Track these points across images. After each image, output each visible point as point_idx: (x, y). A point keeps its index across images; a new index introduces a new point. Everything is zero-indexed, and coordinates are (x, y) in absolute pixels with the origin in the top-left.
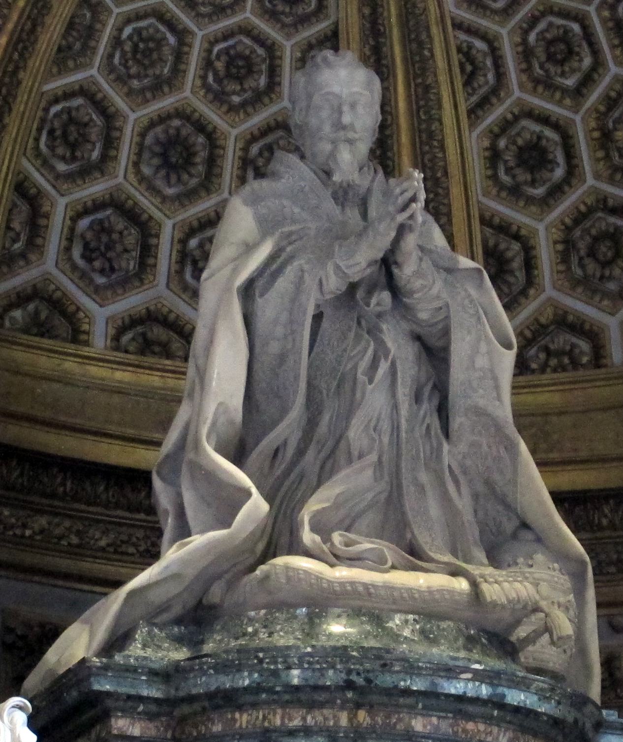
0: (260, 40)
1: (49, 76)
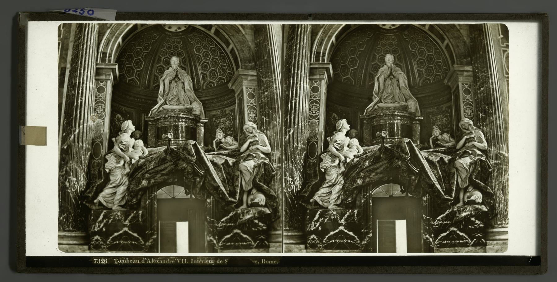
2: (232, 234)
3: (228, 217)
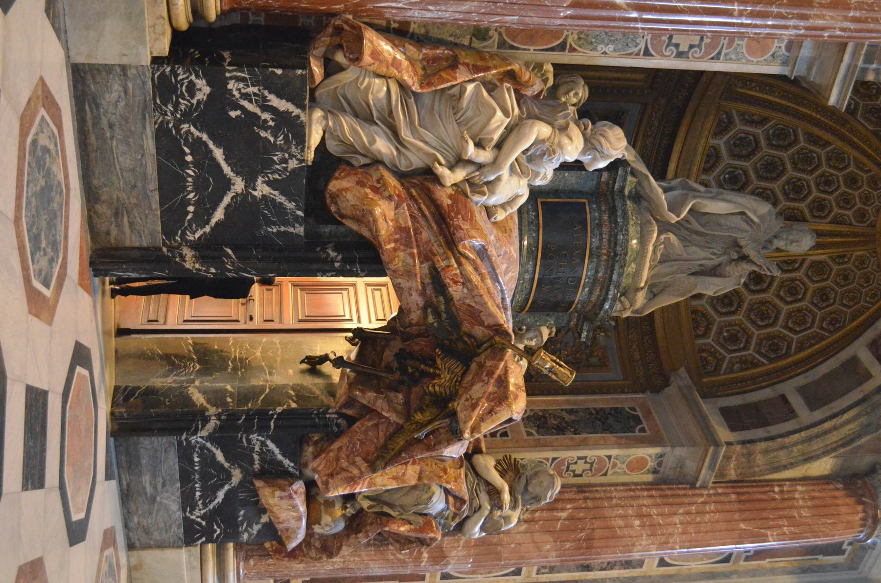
0: (806, 196)
2: (227, 465)
3: (280, 457)
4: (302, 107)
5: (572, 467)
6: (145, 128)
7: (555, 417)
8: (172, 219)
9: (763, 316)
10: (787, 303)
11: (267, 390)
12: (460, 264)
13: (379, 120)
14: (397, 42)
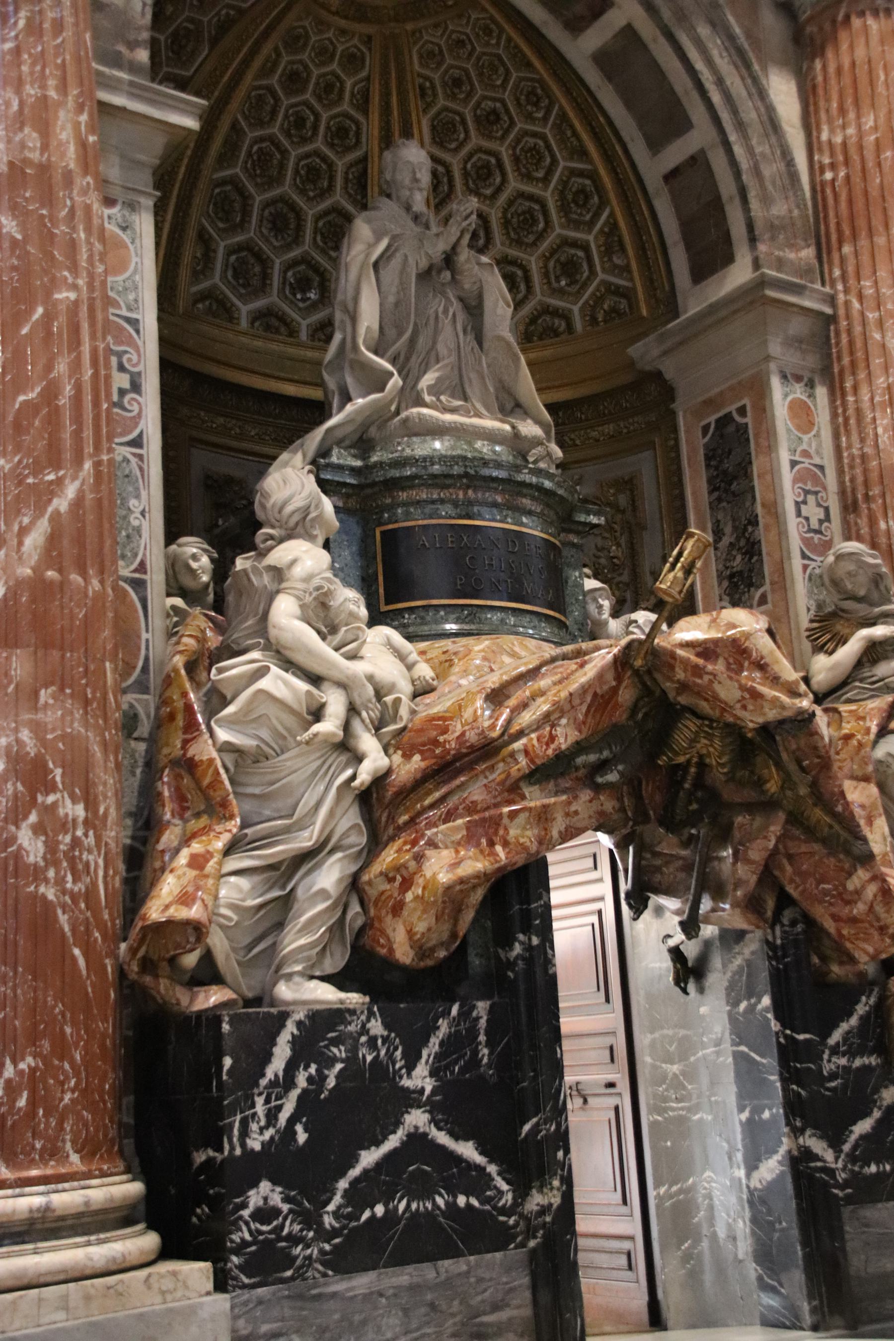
0: (324, 159)
1: (215, 170)
2: (877, 1114)
3: (854, 1021)
4: (284, 1016)
5: (815, 524)
6: (334, 1295)
7: (730, 558)
8: (479, 1233)
9: (529, 220)
10: (504, 180)
11: (743, 1048)
12: (521, 734)
13: (283, 887)
14: (157, 864)
